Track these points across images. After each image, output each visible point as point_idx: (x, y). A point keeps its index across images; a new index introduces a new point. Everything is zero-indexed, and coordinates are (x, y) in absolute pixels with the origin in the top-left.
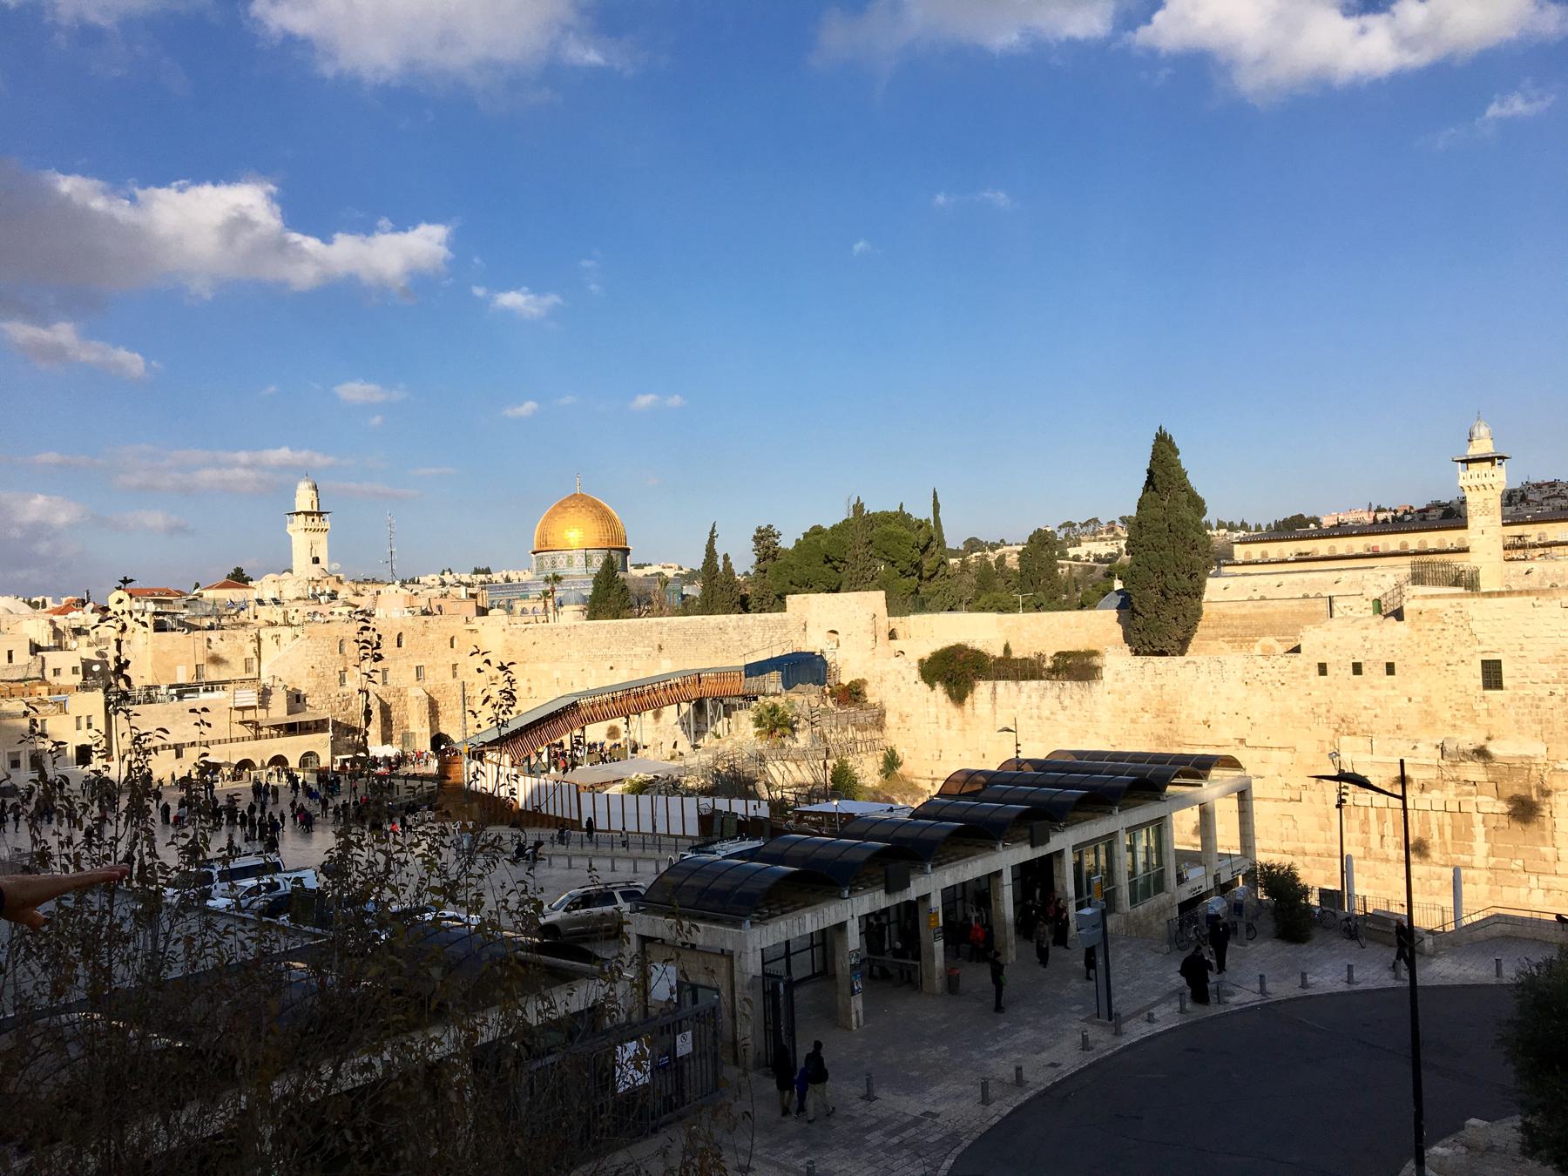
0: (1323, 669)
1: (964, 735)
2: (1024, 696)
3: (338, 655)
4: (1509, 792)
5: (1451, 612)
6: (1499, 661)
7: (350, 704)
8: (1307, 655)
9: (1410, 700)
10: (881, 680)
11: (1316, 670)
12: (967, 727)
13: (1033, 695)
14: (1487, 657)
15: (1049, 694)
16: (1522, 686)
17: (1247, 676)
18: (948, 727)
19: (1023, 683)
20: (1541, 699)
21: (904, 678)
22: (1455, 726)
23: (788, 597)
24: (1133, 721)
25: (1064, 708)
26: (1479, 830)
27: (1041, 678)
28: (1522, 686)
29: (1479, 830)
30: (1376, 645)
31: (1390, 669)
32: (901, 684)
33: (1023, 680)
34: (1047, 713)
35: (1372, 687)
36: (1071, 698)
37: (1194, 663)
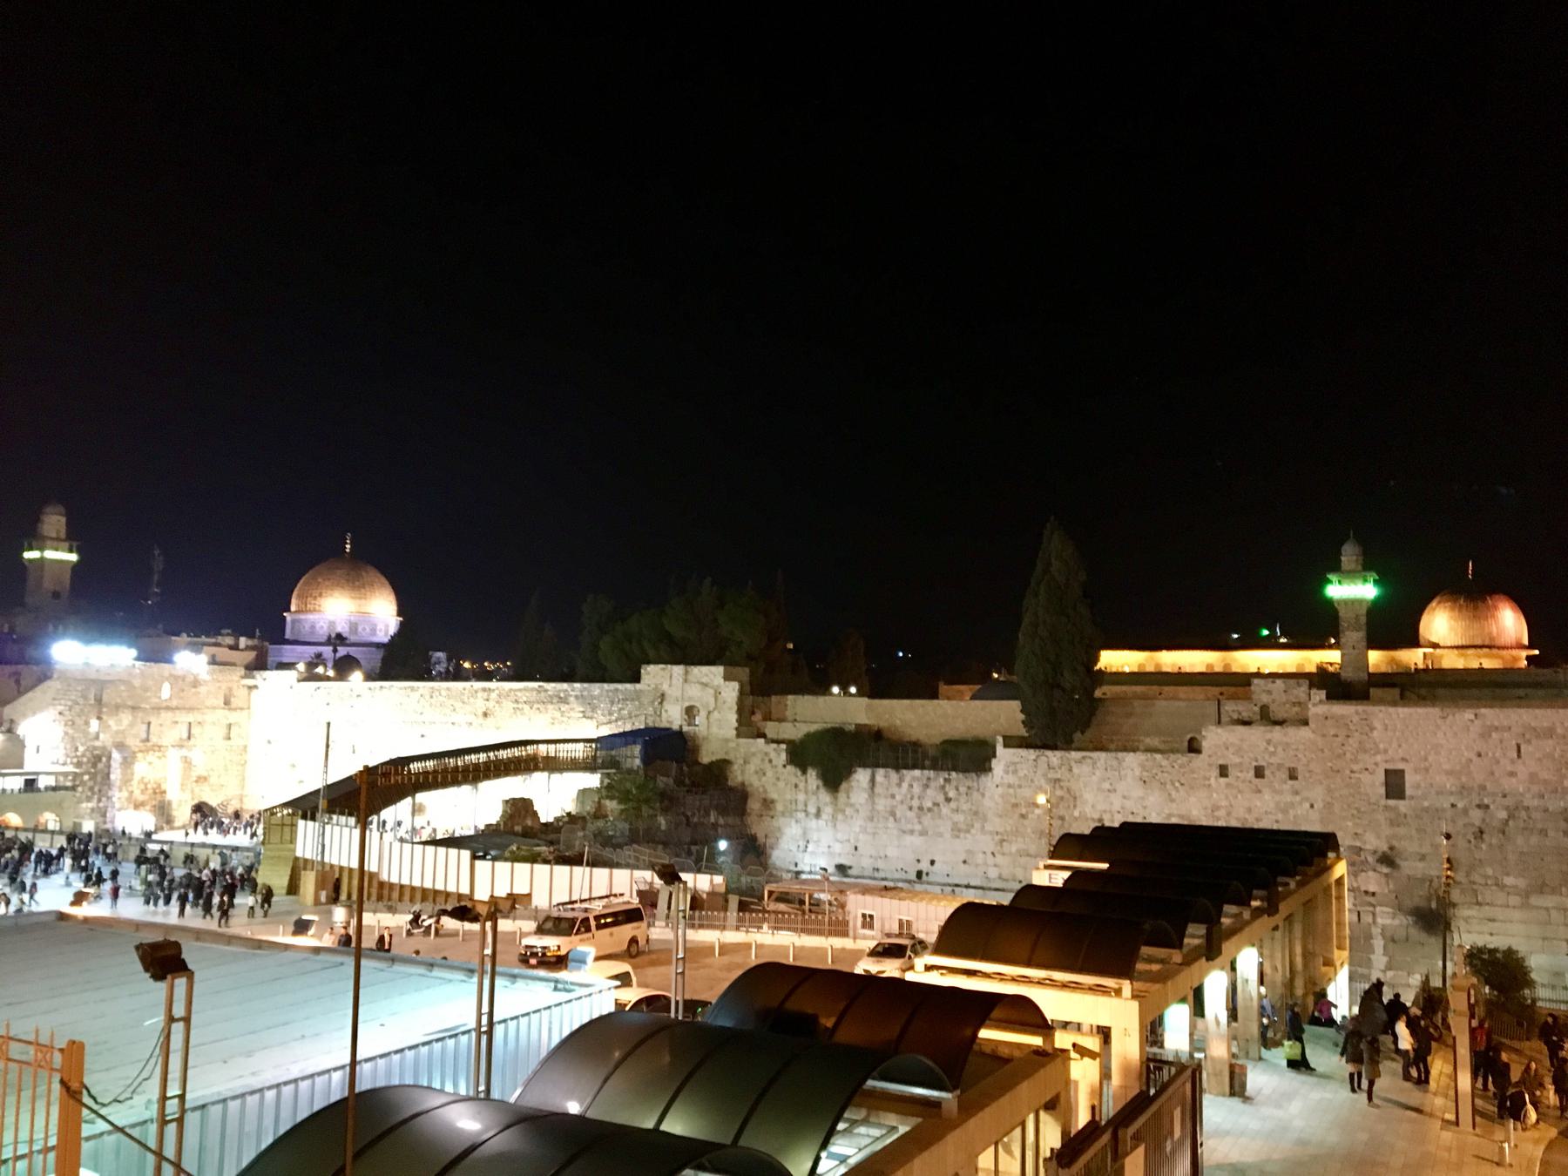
0: (1223, 771)
1: (835, 825)
2: (905, 785)
3: (92, 702)
4: (1409, 903)
5: (1356, 719)
6: (1403, 772)
7: (100, 760)
8: (1210, 756)
9: (1312, 806)
10: (745, 762)
11: (1216, 772)
12: (840, 817)
13: (915, 785)
14: (1391, 766)
15: (933, 784)
16: (1424, 797)
17: (1145, 774)
18: (818, 815)
19: (905, 772)
20: (1444, 810)
21: (770, 761)
22: (1356, 834)
23: (643, 666)
24: (1023, 816)
25: (948, 800)
26: (1378, 943)
27: (923, 768)
28: (1424, 797)
29: (1378, 943)
30: (1280, 749)
31: (1293, 775)
32: (767, 765)
33: (905, 768)
34: (929, 804)
35: (1275, 791)
36: (957, 789)
37: (1091, 758)
